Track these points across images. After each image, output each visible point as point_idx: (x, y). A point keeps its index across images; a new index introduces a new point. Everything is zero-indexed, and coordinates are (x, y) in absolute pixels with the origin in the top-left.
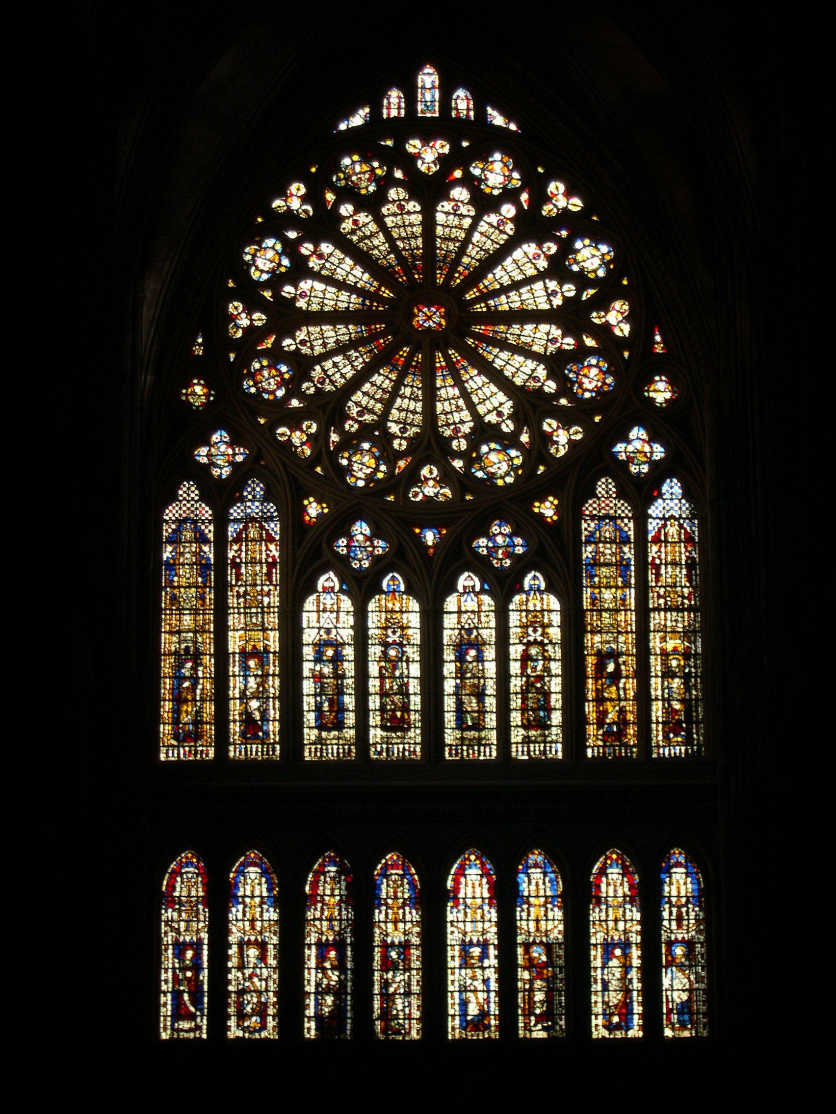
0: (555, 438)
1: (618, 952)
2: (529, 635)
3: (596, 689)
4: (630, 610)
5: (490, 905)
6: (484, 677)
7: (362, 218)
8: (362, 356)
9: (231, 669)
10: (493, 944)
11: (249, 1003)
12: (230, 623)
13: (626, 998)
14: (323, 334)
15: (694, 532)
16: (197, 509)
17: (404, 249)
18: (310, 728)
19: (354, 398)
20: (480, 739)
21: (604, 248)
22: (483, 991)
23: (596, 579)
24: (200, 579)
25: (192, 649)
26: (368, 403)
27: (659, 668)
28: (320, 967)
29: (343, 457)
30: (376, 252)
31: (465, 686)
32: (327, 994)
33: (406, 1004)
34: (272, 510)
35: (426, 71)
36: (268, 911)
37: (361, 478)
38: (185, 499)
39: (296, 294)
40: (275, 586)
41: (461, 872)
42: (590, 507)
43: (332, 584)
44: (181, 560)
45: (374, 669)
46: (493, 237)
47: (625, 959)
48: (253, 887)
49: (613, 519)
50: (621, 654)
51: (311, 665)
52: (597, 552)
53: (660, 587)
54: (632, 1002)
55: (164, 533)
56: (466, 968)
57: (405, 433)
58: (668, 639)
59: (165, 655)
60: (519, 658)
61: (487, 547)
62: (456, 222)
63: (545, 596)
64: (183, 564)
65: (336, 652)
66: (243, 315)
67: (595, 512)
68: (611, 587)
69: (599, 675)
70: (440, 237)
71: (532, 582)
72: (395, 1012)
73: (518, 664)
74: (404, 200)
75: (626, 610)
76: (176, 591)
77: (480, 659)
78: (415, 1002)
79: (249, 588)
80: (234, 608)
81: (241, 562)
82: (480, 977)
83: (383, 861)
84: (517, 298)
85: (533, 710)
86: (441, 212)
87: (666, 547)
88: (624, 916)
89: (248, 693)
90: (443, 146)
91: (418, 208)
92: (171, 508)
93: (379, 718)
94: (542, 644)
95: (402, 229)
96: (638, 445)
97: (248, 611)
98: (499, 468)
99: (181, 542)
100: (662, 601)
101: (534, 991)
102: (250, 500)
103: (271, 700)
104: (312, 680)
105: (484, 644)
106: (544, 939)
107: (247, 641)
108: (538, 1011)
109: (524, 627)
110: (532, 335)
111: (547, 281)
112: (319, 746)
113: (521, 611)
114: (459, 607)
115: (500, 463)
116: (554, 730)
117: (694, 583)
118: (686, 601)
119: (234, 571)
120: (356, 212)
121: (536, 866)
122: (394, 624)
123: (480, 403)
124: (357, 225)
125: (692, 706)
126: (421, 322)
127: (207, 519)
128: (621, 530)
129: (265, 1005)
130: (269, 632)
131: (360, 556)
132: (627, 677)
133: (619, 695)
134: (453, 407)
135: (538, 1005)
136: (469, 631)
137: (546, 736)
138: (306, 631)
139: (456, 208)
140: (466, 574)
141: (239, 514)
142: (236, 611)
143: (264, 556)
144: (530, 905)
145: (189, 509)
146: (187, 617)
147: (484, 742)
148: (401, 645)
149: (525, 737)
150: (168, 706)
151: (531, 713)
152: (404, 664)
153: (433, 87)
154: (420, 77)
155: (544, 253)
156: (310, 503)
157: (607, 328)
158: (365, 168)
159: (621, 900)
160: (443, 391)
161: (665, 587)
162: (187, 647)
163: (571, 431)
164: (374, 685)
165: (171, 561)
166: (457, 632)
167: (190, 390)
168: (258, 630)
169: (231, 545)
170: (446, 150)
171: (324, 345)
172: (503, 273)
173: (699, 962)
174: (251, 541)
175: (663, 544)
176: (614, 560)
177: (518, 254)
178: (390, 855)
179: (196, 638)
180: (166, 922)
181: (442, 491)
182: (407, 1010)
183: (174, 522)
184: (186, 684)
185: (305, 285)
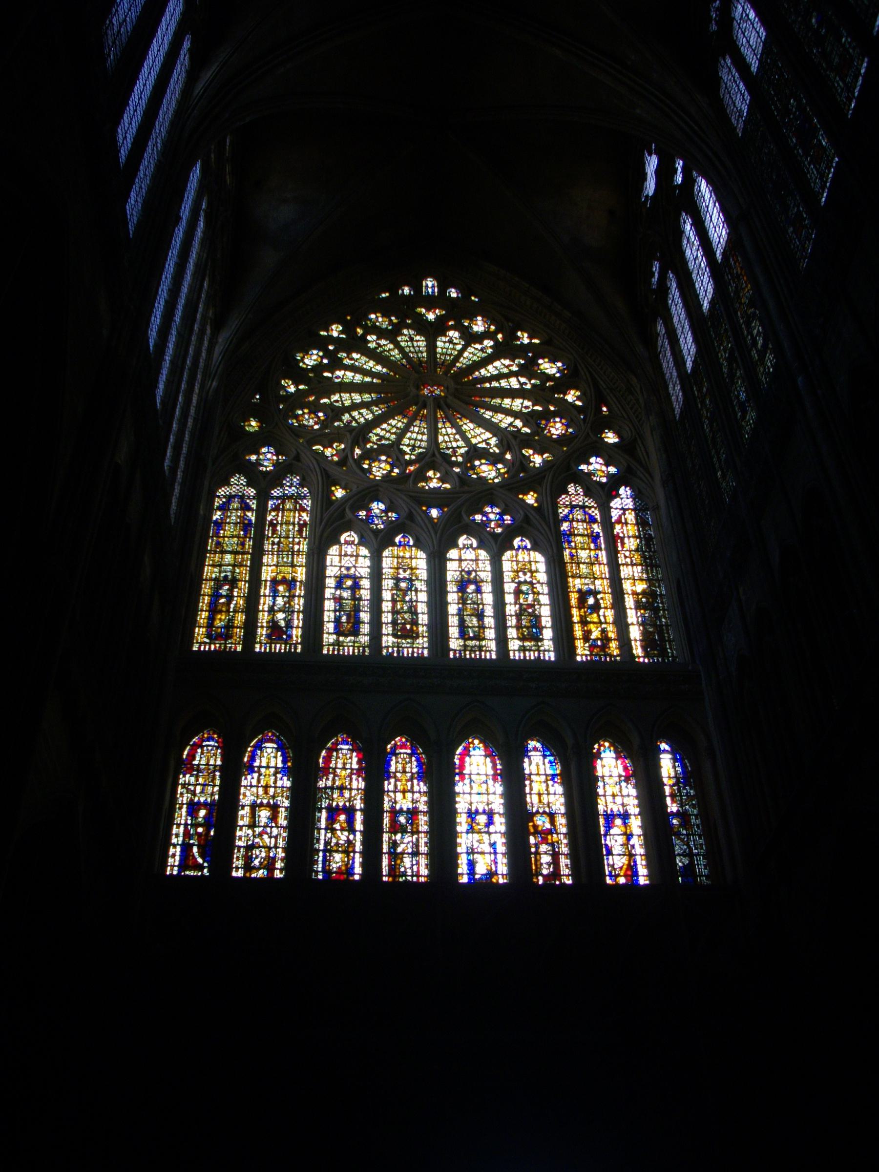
1: (618, 822)
2: (519, 577)
3: (580, 616)
4: (603, 564)
5: (495, 779)
6: (483, 605)
7: (383, 342)
10: (498, 813)
11: (257, 857)
13: (629, 861)
15: (648, 518)
16: (244, 490)
17: (413, 357)
18: (329, 633)
19: (374, 431)
20: (480, 648)
21: (559, 364)
22: (490, 853)
23: (573, 544)
24: (242, 533)
25: (230, 577)
28: (330, 828)
29: (364, 463)
31: (466, 609)
32: (337, 851)
33: (414, 862)
36: (281, 779)
38: (235, 484)
40: (305, 539)
41: (466, 753)
42: (564, 499)
43: (352, 539)
44: (228, 520)
45: (387, 595)
47: (626, 827)
48: (269, 759)
49: (583, 507)
50: (600, 592)
51: (333, 591)
52: (572, 527)
54: (636, 865)
55: (216, 504)
56: (473, 833)
58: (636, 584)
59: (206, 580)
60: (512, 591)
64: (229, 523)
68: (585, 549)
69: (581, 606)
72: (402, 869)
73: (512, 596)
75: (600, 564)
76: (221, 540)
77: (478, 591)
78: (423, 861)
79: (282, 539)
81: (278, 523)
82: (487, 842)
83: (393, 742)
85: (525, 627)
88: (621, 792)
89: (276, 608)
91: (423, 338)
92: (223, 489)
93: (391, 629)
94: (531, 583)
96: (598, 467)
99: (229, 509)
100: (628, 560)
101: (540, 854)
103: (296, 613)
104: (332, 601)
105: (482, 581)
106: (547, 810)
107: (278, 573)
108: (545, 872)
111: (519, 378)
112: (337, 647)
114: (460, 557)
116: (546, 643)
120: (378, 339)
121: (535, 749)
122: (405, 565)
125: (663, 630)
128: (589, 515)
129: (273, 860)
132: (606, 608)
133: (600, 620)
135: (545, 866)
136: (469, 573)
137: (539, 647)
143: (297, 520)
144: (532, 781)
147: (484, 649)
149: (520, 646)
150: (205, 615)
151: (525, 629)
152: (413, 593)
153: (433, 286)
156: (337, 489)
159: (617, 779)
162: (226, 576)
164: (387, 606)
165: (219, 521)
166: (458, 573)
169: (270, 513)
172: (486, 372)
173: (695, 831)
177: (497, 364)
178: (399, 738)
179: (235, 570)
180: (184, 786)
182: (415, 868)
183: (225, 497)
184: (222, 600)
185: (338, 373)
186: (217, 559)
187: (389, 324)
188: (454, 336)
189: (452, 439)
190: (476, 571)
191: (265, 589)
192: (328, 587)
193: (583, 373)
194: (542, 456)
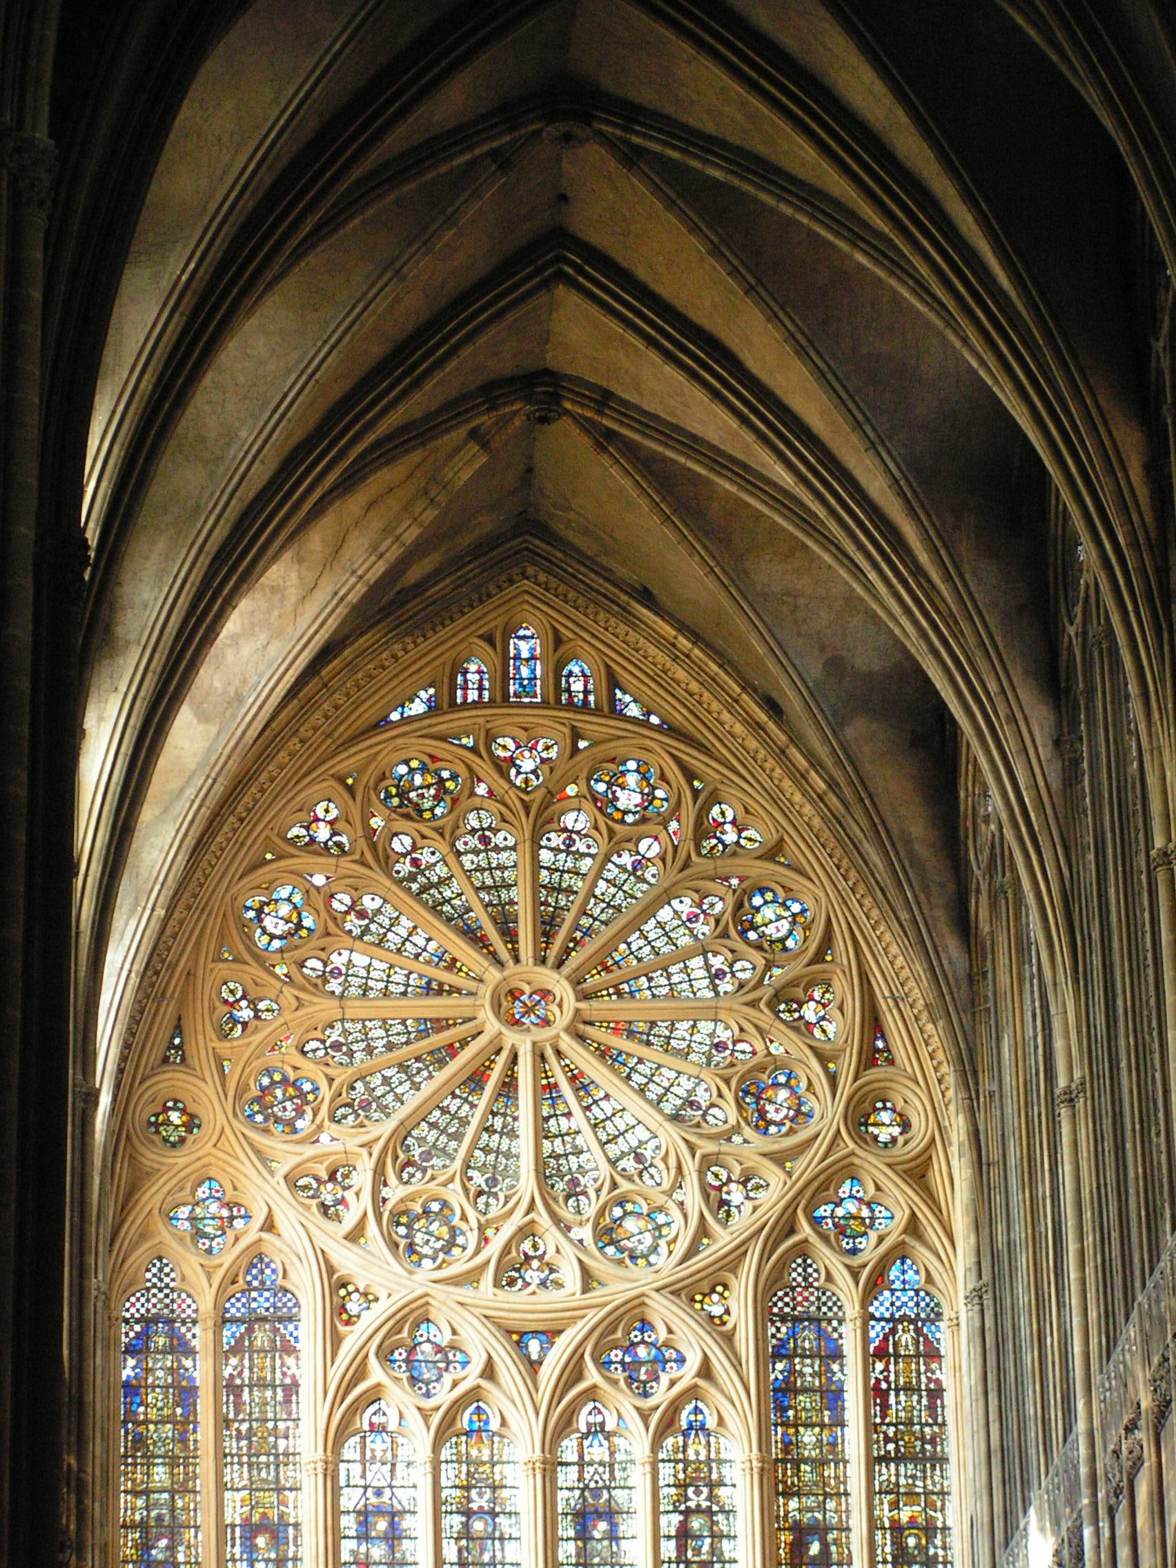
0: (725, 1196)
2: (687, 1499)
8: (427, 1067)
9: (229, 1549)
12: (227, 1478)
14: (367, 1034)
16: (173, 1301)
17: (490, 904)
19: (415, 1133)
23: (791, 1413)
24: (179, 1411)
25: (167, 1518)
26: (437, 1139)
27: (888, 1549)
29: (398, 1224)
30: (447, 908)
34: (290, 1304)
35: (521, 633)
37: (426, 1256)
38: (154, 1286)
39: (324, 972)
43: (383, 1419)
44: (150, 1381)
46: (625, 888)
51: (352, 1544)
52: (791, 1371)
53: (889, 1425)
57: (495, 1186)
59: (124, 1526)
60: (673, 1533)
61: (622, 1362)
62: (569, 865)
63: (712, 1439)
65: (392, 1524)
66: (244, 1003)
67: (787, 1310)
68: (813, 1426)
70: (544, 887)
71: (692, 1417)
73: (673, 1543)
74: (489, 828)
77: (613, 1536)
79: (255, 1424)
80: (232, 1456)
84: (663, 981)
86: (545, 847)
87: (896, 1363)
90: (547, 748)
92: (133, 1299)
94: (709, 1512)
95: (486, 874)
96: (851, 1207)
97: (254, 1459)
98: (639, 1241)
100: (891, 1447)
102: (255, 1289)
107: (252, 1508)
109: (682, 1486)
110: (688, 1037)
111: (710, 955)
113: (677, 1461)
114: (581, 1456)
115: (641, 1233)
117: (940, 1420)
118: (928, 1447)
119: (231, 1397)
120: (415, 848)
123: (608, 1142)
124: (418, 866)
126: (517, 1017)
127: (189, 1316)
128: (829, 1338)
130: (286, 1493)
131: (426, 1376)
134: (568, 1146)
136: (596, 1493)
138: (345, 1491)
139: (570, 843)
140: (591, 1405)
141: (238, 1310)
142: (236, 1459)
145: (160, 1301)
146: (161, 1469)
148: (494, 1514)
152: (497, 1542)
153: (533, 658)
154: (512, 641)
155: (703, 912)
156: (349, 1294)
157: (803, 1028)
158: (430, 780)
160: (552, 1121)
161: (895, 1425)
162: (159, 1518)
163: (749, 1185)
166: (577, 1493)
167: (161, 1118)
168: (272, 1489)
169: (227, 1359)
170: (553, 753)
171: (369, 1050)
172: (642, 942)
174: (258, 1352)
175: (892, 1359)
176: (817, 1383)
177: (665, 914)
181: (551, 1277)
183: (137, 1321)
185: (338, 960)
186: (139, 1476)
187: (438, 798)
188: (578, 827)
189: (569, 1149)
190: (608, 1488)
191: (233, 1546)
192: (345, 1537)
193: (841, 944)
194: (745, 1187)
